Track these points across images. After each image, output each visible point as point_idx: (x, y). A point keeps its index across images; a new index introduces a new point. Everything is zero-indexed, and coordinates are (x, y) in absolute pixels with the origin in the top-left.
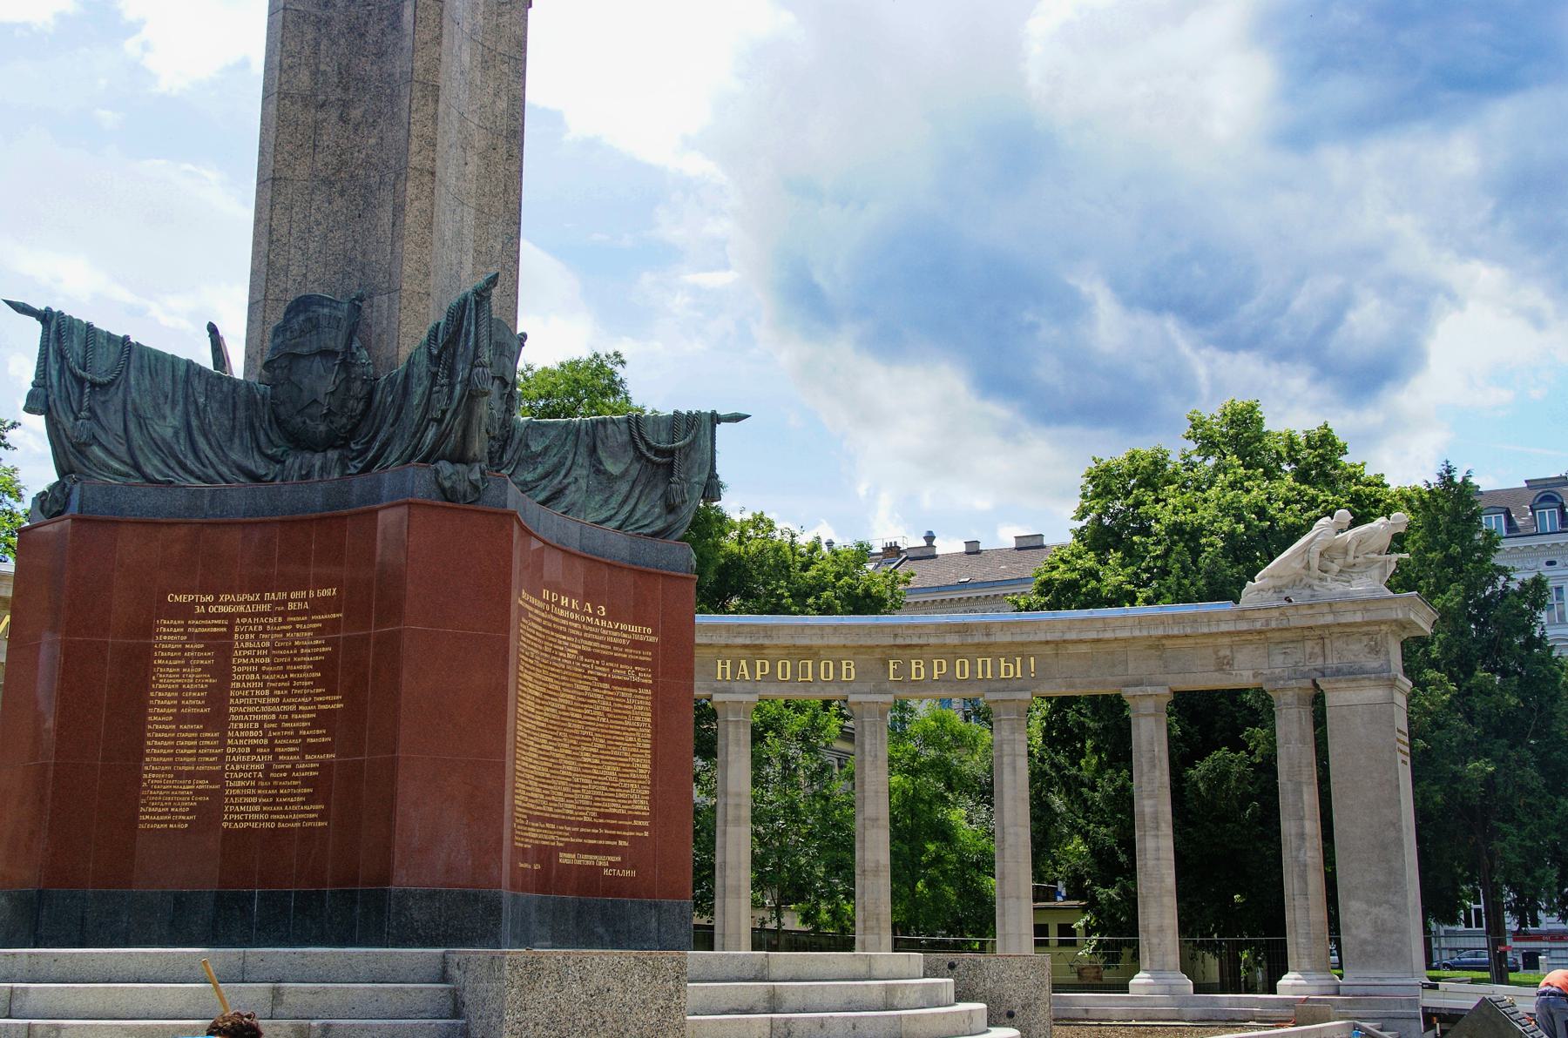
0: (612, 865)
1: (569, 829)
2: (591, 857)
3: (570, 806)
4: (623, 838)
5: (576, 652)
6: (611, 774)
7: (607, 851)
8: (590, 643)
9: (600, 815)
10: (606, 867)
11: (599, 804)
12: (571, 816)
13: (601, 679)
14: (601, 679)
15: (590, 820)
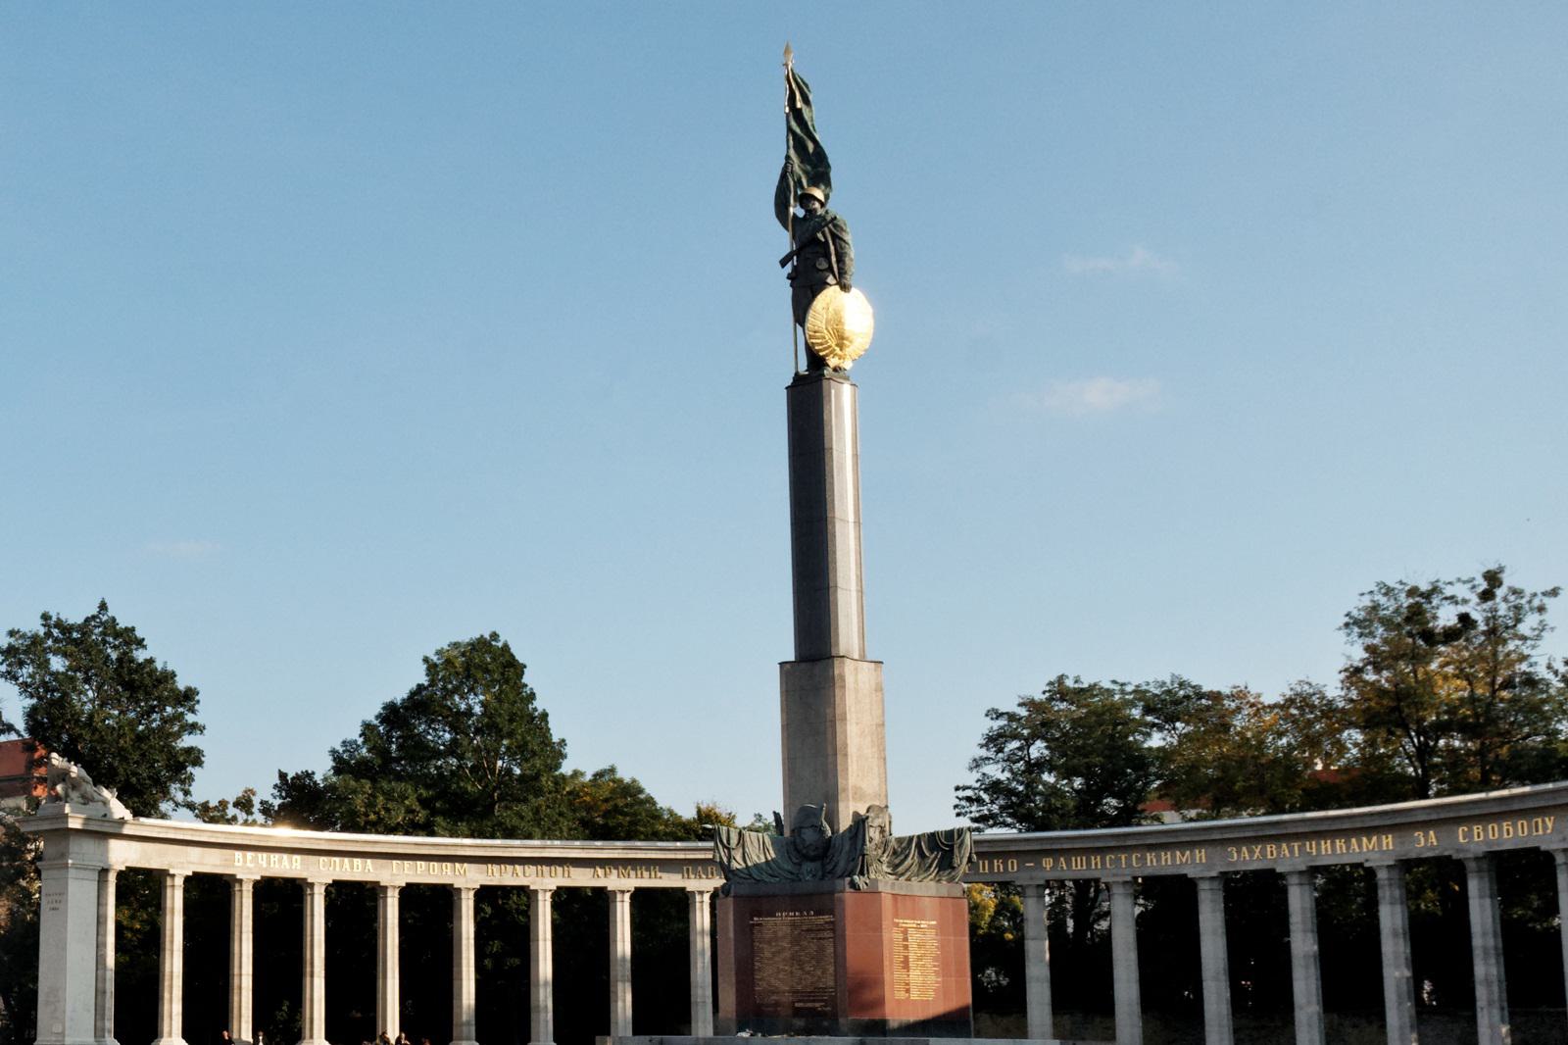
7: (819, 1001)
14: (813, 939)
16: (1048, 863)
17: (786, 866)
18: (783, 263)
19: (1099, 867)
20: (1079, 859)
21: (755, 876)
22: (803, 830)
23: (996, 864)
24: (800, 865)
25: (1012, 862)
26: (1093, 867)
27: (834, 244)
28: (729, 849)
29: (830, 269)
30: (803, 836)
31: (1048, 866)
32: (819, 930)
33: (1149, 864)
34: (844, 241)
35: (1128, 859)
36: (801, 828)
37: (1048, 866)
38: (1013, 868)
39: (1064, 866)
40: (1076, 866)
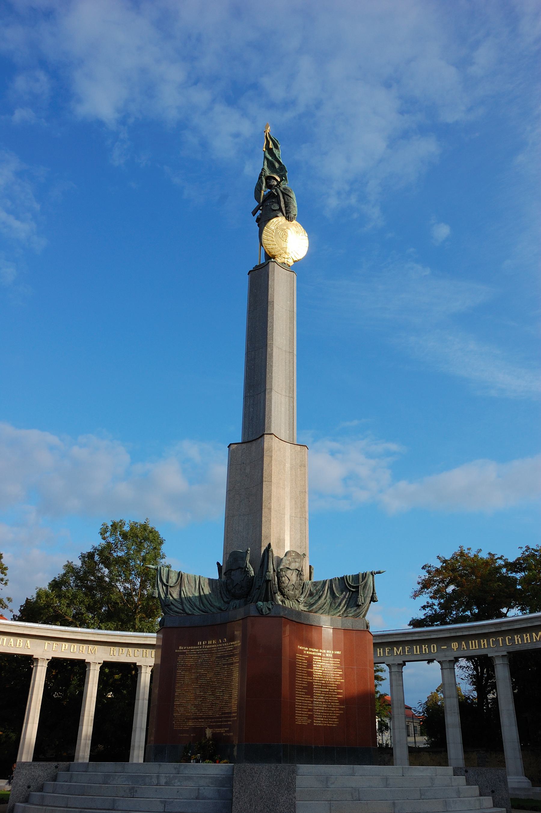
0: (226, 731)
1: (210, 720)
2: (219, 729)
3: (211, 712)
4: (230, 721)
5: (215, 658)
6: (227, 698)
7: (225, 726)
8: (220, 653)
9: (223, 714)
10: (224, 732)
11: (222, 710)
12: (211, 715)
13: (224, 665)
14: (224, 665)
15: (219, 716)
16: (455, 645)
17: (217, 604)
18: (254, 213)
19: (486, 647)
20: (473, 641)
21: (187, 611)
22: (233, 572)
23: (424, 648)
24: (228, 603)
25: (434, 646)
26: (483, 647)
27: (284, 198)
28: (167, 586)
29: (280, 210)
30: (232, 577)
31: (455, 648)
32: (228, 656)
33: (517, 643)
34: (290, 197)
35: (504, 640)
36: (232, 570)
37: (455, 648)
38: (434, 651)
39: (465, 647)
40: (472, 647)
